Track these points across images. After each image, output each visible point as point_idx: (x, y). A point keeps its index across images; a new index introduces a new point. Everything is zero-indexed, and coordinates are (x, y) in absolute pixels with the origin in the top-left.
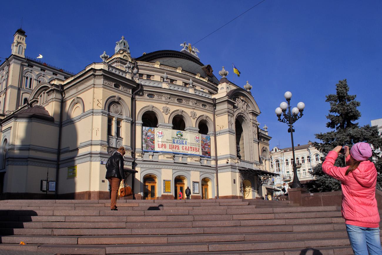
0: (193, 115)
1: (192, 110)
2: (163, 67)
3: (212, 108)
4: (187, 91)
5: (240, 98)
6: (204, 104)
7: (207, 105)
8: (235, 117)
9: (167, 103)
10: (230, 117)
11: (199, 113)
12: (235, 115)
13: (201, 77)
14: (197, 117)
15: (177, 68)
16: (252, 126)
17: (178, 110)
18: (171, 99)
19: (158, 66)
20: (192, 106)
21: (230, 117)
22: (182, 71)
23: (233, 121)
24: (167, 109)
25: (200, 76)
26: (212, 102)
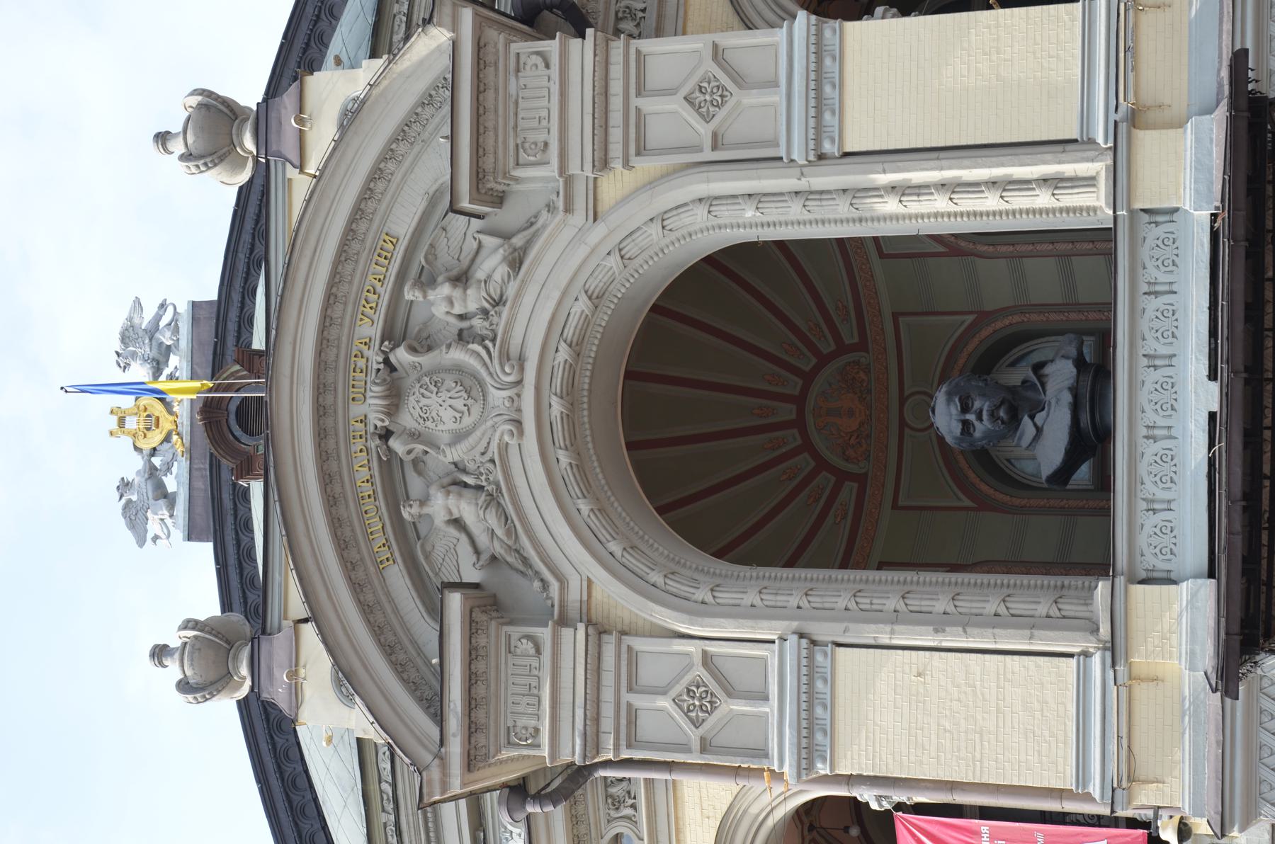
16: (647, 166)
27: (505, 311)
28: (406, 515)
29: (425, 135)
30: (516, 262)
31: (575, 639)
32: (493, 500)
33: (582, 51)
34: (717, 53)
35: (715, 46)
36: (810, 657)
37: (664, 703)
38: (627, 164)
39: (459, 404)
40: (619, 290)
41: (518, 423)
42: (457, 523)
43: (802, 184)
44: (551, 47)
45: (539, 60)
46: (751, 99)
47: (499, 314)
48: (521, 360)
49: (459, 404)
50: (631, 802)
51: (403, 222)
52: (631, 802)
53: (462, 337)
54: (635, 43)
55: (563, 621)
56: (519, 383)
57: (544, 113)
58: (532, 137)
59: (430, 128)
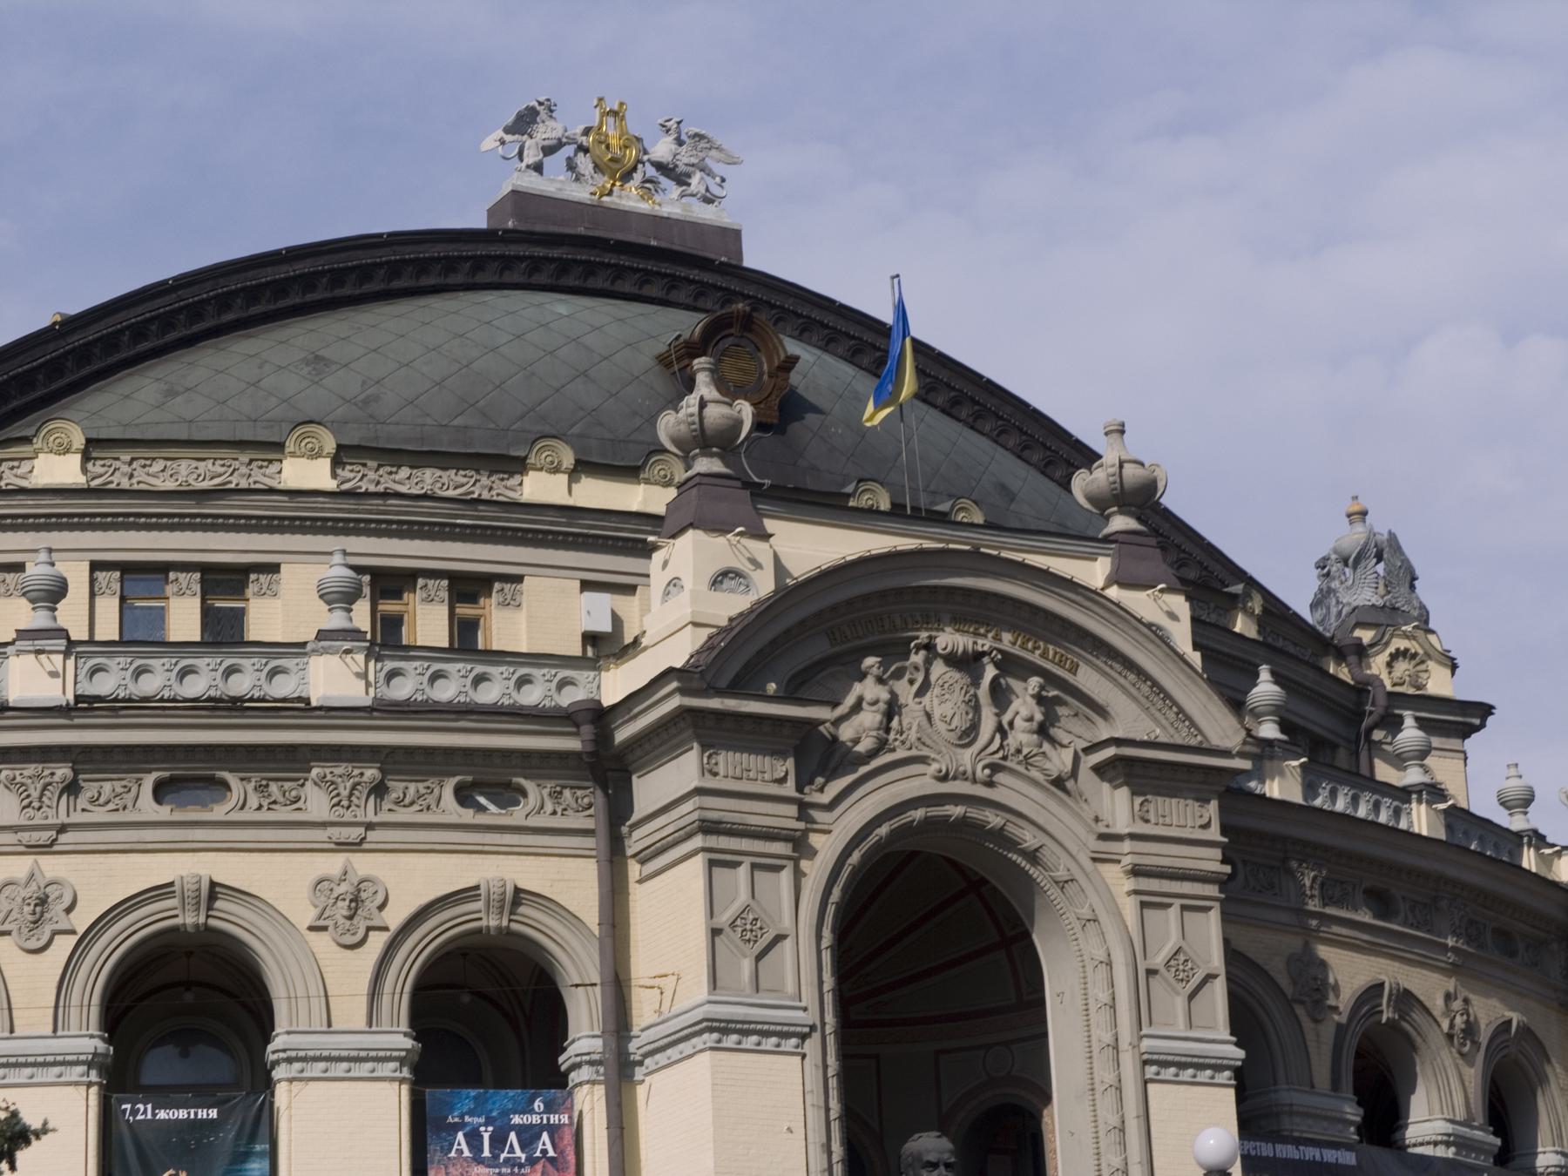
0: (343, 908)
1: (332, 864)
2: (120, 471)
3: (580, 809)
4: (283, 688)
5: (929, 647)
6: (488, 779)
7: (529, 785)
8: (816, 871)
9: (44, 837)
10: (743, 872)
11: (411, 879)
12: (827, 847)
13: (584, 467)
14: (395, 917)
15: (279, 446)
16: (1129, 907)
17: (162, 891)
18: (90, 790)
19: (56, 467)
20: (324, 825)
21: (743, 872)
22: (337, 462)
23: (798, 906)
24: (43, 901)
25: (568, 460)
26: (572, 744)
27: (1021, 769)
28: (870, 661)
29: (1153, 710)
30: (1059, 783)
31: (784, 817)
32: (882, 746)
33: (1211, 861)
34: (1210, 977)
35: (1215, 976)
36: (793, 1035)
37: (743, 896)
38: (1136, 892)
39: (955, 722)
40: (1033, 872)
41: (943, 778)
42: (857, 707)
43: (1124, 1044)
44: (1214, 833)
45: (1205, 820)
46: (1180, 1002)
47: (1019, 763)
48: (990, 784)
49: (955, 722)
50: (559, 810)
51: (1088, 679)
52: (559, 810)
53: (1001, 730)
54: (1217, 905)
55: (804, 808)
56: (974, 781)
57: (1168, 821)
58: (1152, 807)
59: (1158, 715)
